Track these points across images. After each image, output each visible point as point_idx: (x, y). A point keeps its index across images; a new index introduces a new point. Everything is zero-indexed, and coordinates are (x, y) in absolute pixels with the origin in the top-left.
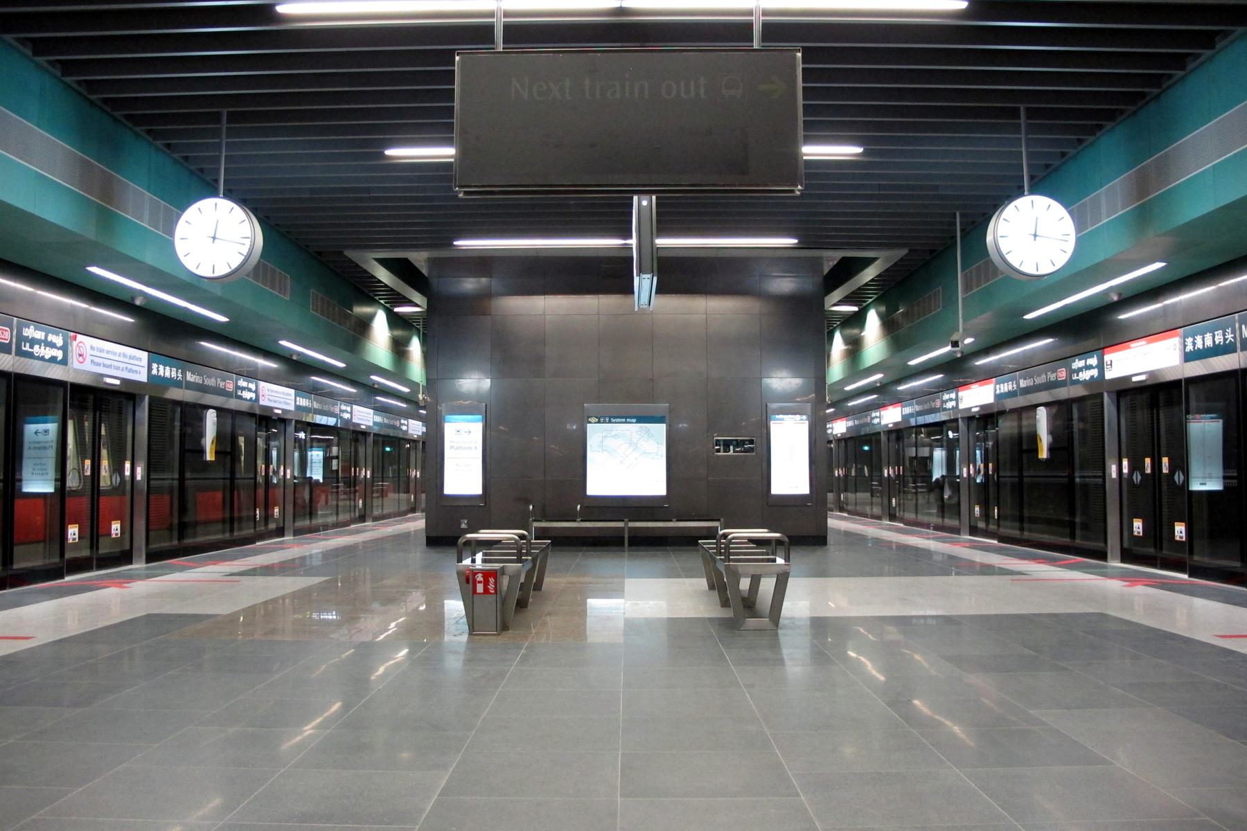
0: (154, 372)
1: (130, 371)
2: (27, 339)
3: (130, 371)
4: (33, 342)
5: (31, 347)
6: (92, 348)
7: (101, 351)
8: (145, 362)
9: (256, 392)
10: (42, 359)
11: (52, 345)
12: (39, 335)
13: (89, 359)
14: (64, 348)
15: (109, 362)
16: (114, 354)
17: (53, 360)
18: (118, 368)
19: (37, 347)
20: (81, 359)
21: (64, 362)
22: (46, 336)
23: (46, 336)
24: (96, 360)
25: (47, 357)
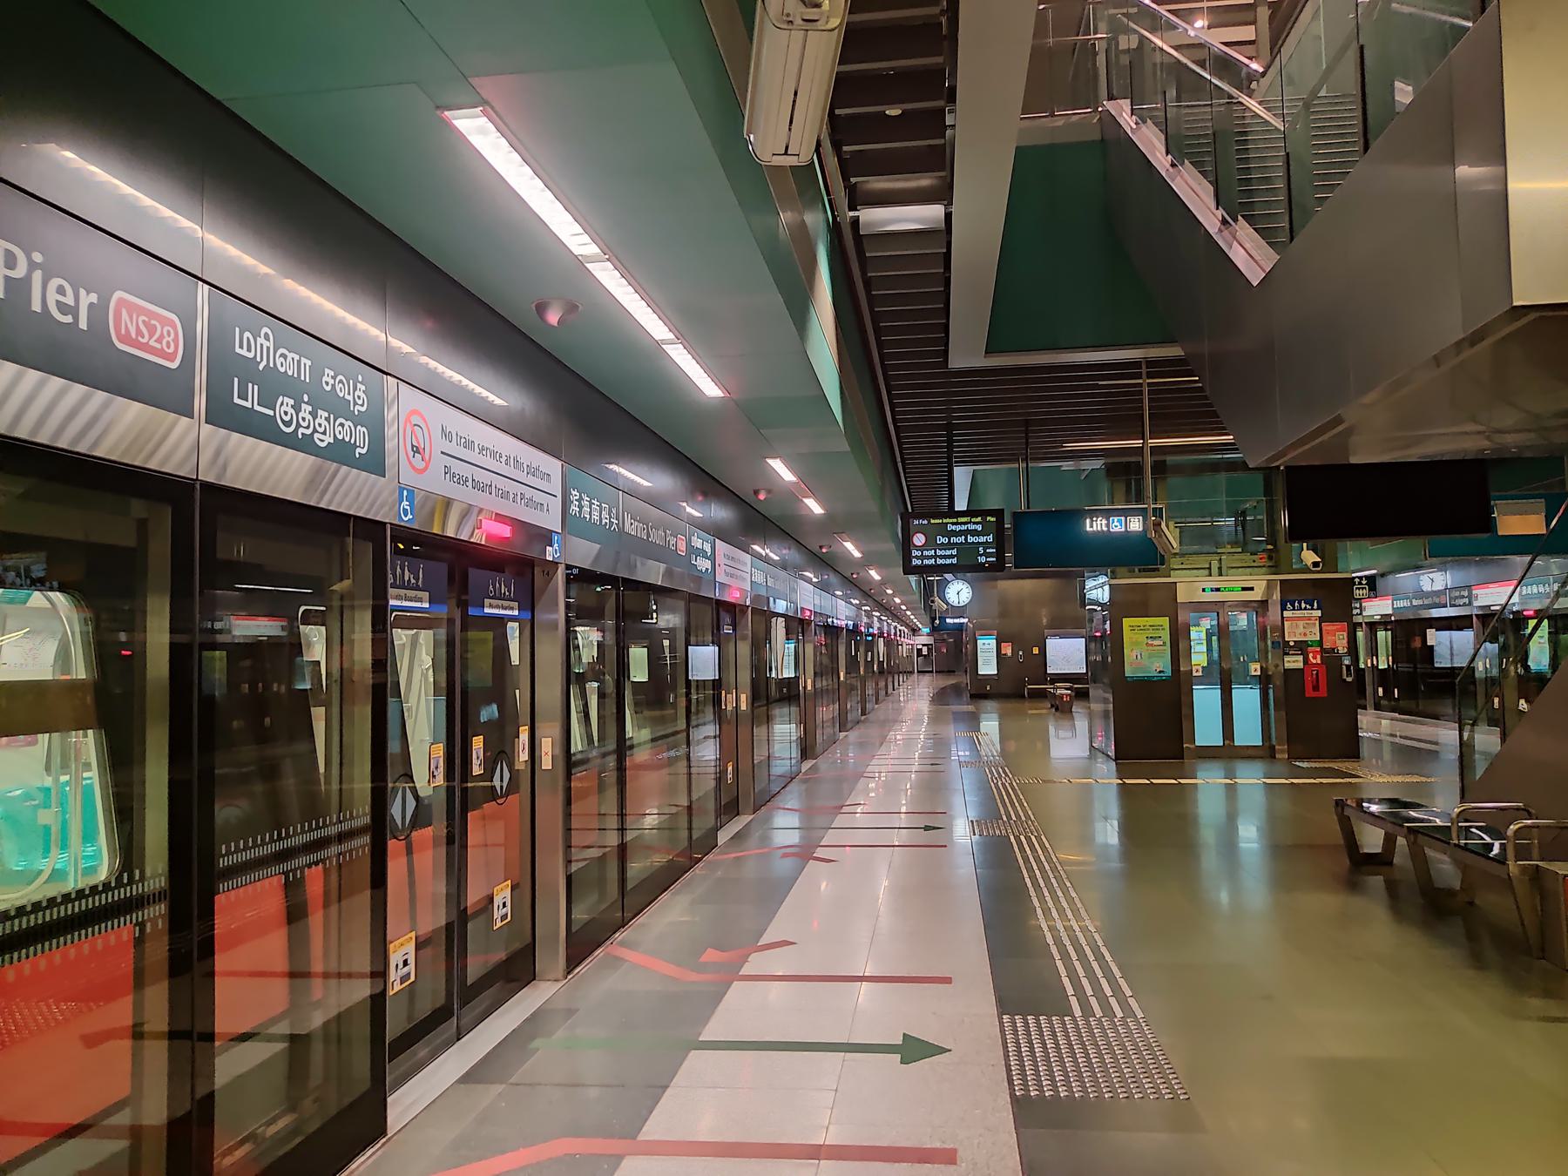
0: (574, 508)
1: (530, 503)
2: (248, 371)
3: (530, 503)
4: (274, 385)
5: (268, 400)
6: (446, 435)
7: (469, 445)
8: (556, 487)
9: (713, 558)
10: (304, 444)
11: (339, 409)
12: (290, 363)
13: (439, 462)
14: (375, 423)
15: (485, 478)
16: (495, 455)
17: (340, 453)
18: (504, 495)
19: (285, 405)
20: (418, 461)
21: (375, 463)
22: (317, 373)
23: (317, 373)
24: (458, 467)
25: (323, 441)
